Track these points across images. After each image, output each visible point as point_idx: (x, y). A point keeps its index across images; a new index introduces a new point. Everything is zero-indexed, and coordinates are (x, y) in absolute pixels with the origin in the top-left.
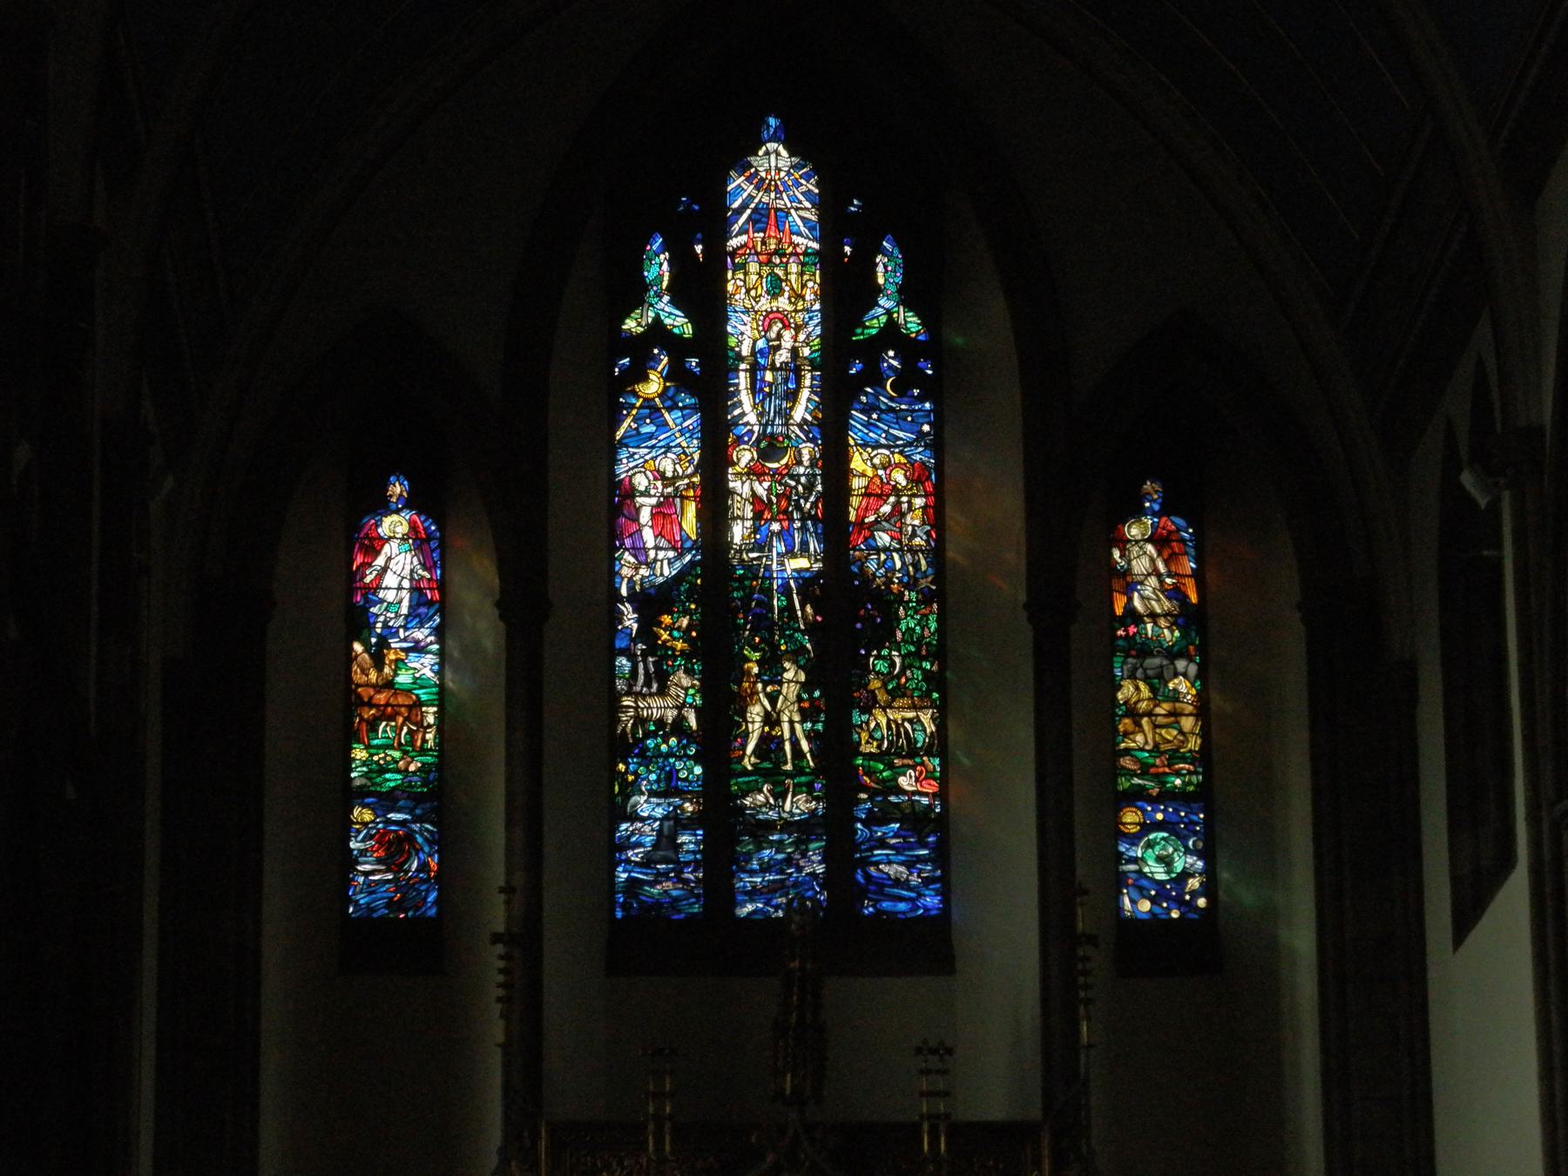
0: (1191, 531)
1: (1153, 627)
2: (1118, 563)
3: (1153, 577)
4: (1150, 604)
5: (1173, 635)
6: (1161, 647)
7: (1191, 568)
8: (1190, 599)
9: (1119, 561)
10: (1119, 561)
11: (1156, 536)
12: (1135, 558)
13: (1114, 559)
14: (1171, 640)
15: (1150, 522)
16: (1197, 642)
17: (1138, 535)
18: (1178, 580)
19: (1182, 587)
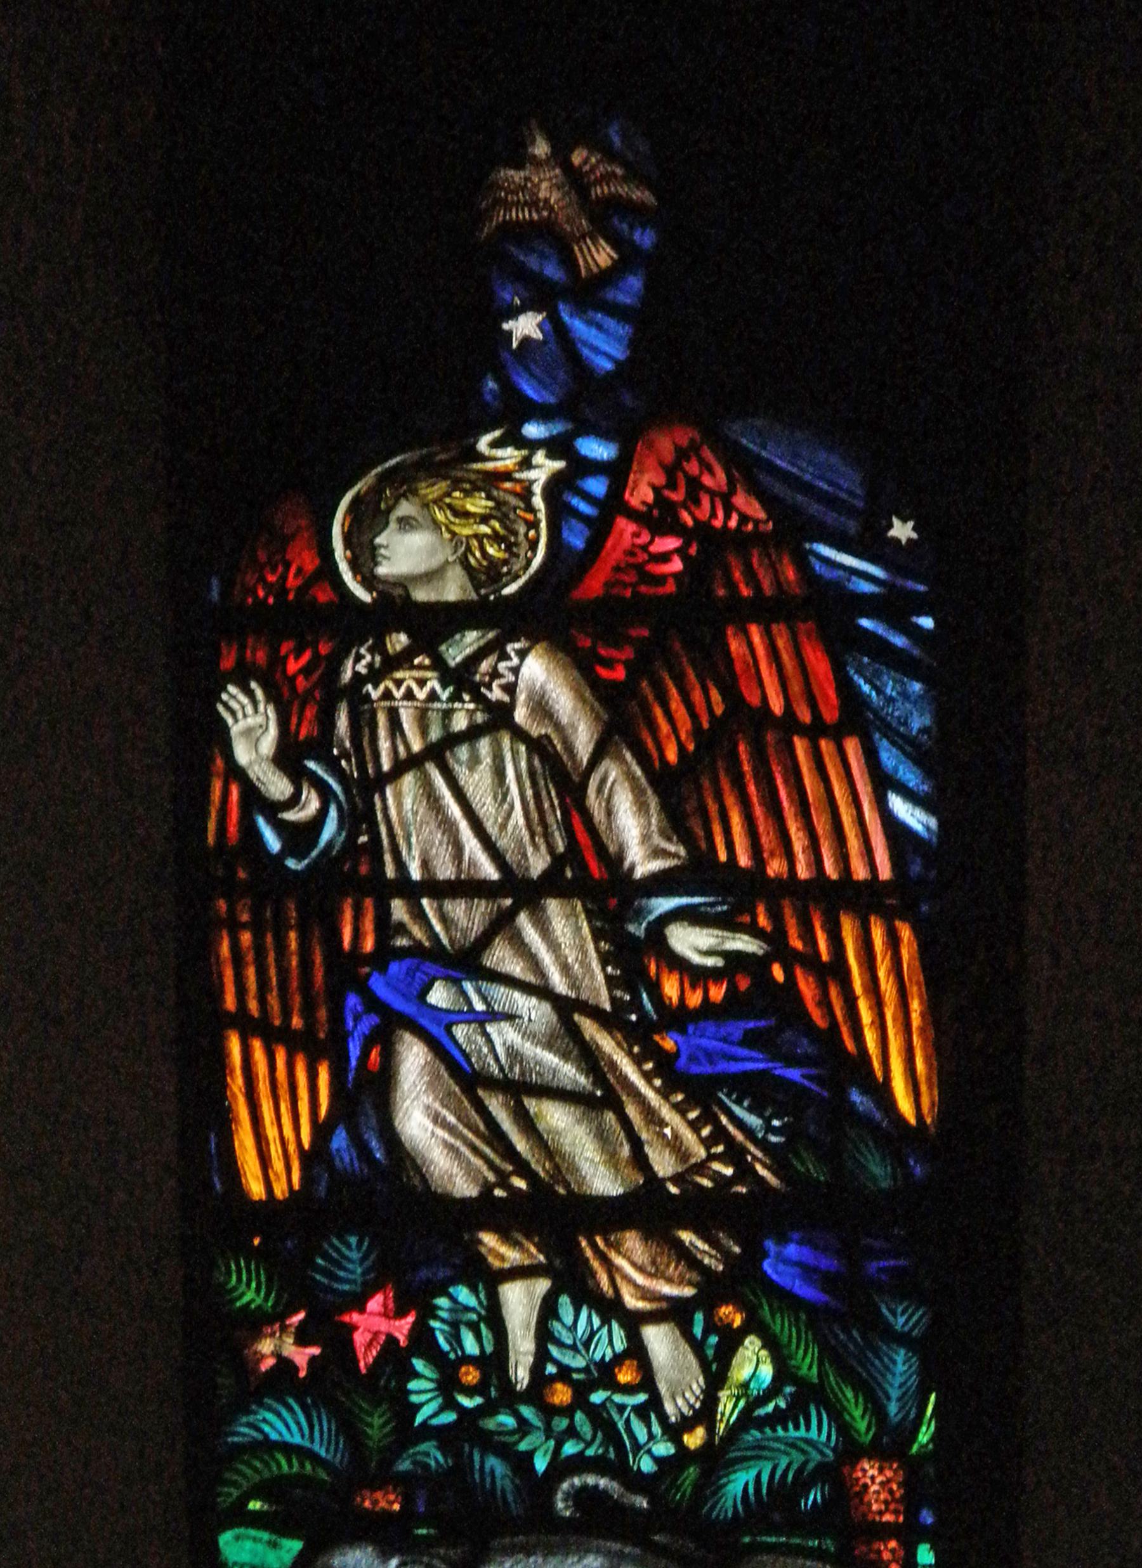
0: (902, 531)
1: (548, 1310)
2: (272, 809)
3: (553, 906)
4: (527, 1123)
5: (716, 1379)
6: (620, 1469)
7: (894, 828)
8: (883, 1093)
9: (278, 786)
10: (278, 786)
11: (594, 585)
12: (413, 762)
13: (236, 773)
14: (706, 1413)
15: (544, 468)
16: (924, 1436)
17: (431, 576)
18: (776, 939)
19: (807, 987)
